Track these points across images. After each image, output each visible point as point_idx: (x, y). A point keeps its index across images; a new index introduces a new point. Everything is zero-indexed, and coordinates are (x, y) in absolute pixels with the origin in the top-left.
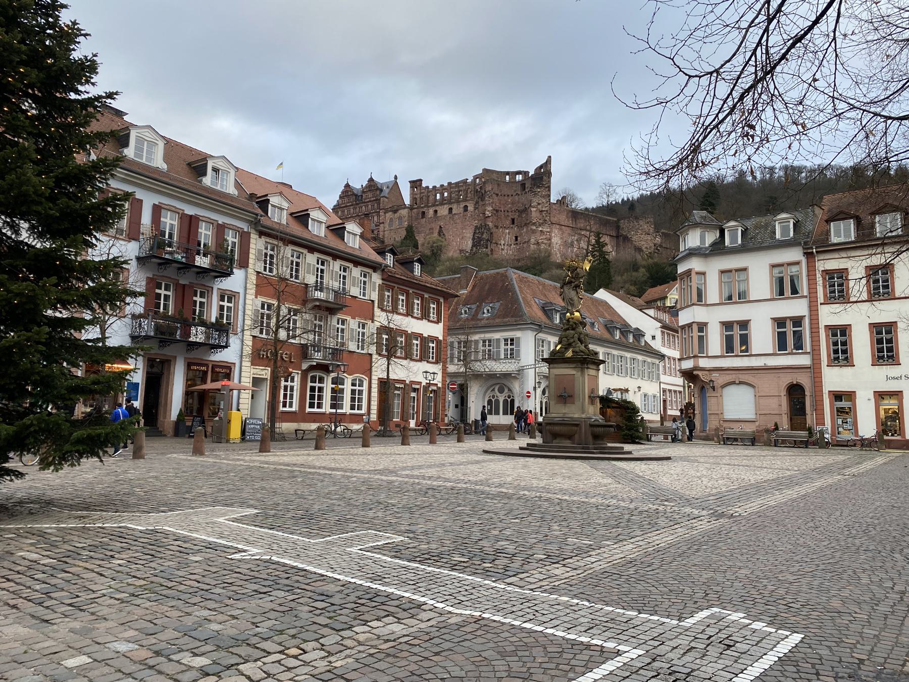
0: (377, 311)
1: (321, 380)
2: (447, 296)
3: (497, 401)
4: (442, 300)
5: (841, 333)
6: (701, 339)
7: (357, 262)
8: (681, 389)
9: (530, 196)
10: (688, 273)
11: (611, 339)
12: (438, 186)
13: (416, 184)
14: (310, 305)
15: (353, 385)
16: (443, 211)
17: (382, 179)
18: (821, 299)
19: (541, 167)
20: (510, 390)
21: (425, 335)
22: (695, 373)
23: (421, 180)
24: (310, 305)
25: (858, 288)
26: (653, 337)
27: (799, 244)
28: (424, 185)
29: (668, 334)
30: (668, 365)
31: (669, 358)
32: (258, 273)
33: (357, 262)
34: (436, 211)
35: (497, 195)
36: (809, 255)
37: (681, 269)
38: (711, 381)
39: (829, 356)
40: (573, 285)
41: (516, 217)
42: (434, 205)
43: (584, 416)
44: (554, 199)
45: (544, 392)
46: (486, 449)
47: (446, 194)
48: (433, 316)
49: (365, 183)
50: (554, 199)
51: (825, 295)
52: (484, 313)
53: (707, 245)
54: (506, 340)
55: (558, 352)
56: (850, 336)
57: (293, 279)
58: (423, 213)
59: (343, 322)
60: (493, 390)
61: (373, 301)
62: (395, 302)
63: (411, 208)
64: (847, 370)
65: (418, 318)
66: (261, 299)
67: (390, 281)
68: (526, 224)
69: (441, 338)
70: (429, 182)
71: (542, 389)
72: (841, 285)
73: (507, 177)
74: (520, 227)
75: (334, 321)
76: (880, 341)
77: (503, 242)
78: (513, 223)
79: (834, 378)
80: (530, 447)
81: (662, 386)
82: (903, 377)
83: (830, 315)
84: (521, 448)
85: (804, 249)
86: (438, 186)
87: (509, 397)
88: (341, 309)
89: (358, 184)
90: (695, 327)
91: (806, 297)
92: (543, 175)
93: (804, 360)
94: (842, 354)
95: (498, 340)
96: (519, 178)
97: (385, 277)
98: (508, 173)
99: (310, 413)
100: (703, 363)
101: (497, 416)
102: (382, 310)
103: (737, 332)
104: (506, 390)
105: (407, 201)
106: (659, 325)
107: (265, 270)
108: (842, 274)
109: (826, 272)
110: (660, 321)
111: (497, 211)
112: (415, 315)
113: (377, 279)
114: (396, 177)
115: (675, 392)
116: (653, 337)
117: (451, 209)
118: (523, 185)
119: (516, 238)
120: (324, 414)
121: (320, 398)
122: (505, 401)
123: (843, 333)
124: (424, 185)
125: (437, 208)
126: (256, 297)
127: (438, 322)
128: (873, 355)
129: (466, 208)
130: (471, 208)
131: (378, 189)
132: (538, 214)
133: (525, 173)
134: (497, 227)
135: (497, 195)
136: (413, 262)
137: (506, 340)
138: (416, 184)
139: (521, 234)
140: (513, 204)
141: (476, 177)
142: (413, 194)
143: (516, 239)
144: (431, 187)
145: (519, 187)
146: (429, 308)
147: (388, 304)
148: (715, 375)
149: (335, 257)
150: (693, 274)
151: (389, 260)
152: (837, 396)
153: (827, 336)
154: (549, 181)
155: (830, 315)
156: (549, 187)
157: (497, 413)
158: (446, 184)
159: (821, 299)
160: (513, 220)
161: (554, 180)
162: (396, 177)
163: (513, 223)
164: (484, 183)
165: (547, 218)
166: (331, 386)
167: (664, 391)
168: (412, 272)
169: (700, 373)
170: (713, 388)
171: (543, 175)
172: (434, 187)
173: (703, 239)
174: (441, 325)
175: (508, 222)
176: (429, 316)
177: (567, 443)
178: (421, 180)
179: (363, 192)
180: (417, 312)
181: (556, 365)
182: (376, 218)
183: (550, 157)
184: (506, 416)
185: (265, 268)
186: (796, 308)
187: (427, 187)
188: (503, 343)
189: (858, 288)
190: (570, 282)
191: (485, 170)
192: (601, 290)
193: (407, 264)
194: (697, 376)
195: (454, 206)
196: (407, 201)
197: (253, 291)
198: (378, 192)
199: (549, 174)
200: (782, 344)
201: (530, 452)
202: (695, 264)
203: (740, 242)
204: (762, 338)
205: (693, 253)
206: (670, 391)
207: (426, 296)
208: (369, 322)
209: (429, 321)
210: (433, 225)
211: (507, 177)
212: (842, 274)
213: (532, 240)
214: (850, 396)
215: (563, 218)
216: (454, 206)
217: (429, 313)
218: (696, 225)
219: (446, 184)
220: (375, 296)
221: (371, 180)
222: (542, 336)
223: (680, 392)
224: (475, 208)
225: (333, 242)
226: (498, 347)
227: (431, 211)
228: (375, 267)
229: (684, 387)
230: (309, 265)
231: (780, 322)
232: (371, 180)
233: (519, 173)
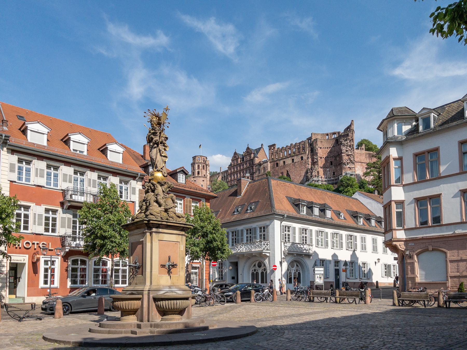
11: (298, 216)
16: (289, 161)
23: (274, 145)
34: (284, 162)
35: (321, 148)
41: (333, 160)
49: (245, 150)
58: (277, 164)
60: (255, 265)
74: (336, 166)
78: (332, 164)
89: (241, 151)
95: (255, 228)
104: (263, 265)
117: (293, 160)
119: (334, 173)
125: (285, 160)
130: (305, 158)
135: (321, 148)
136: (177, 173)
139: (337, 170)
143: (334, 174)
160: (331, 163)
163: (332, 164)
165: (352, 159)
182: (251, 171)
195: (295, 158)
210: (283, 170)
216: (295, 158)
221: (248, 148)
222: (284, 223)
227: (281, 163)
230: (65, 175)
232: (248, 148)
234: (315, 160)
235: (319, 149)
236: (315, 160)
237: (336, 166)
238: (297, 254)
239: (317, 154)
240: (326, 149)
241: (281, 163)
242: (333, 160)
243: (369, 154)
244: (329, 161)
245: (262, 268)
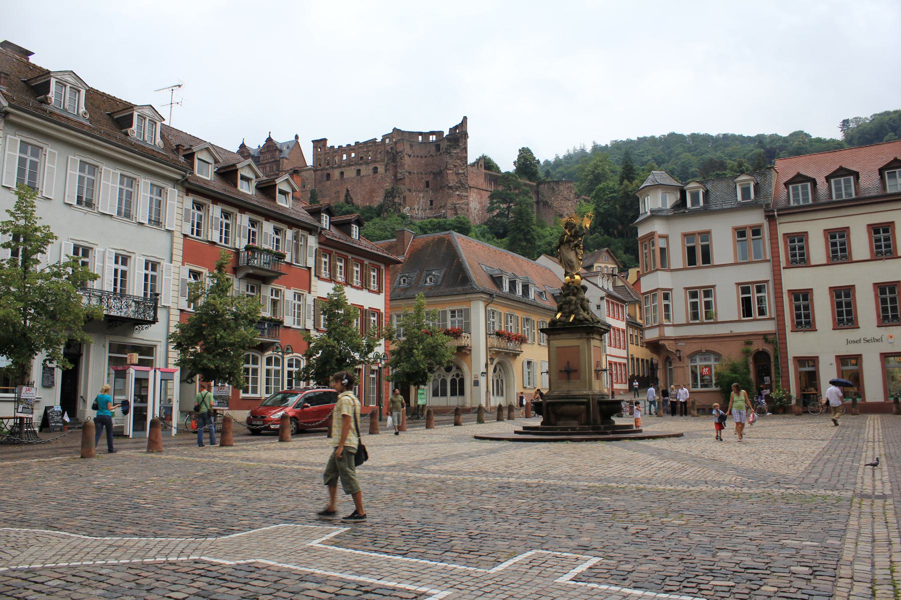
0: (313, 278)
1: (255, 361)
2: (388, 262)
3: (444, 382)
4: (383, 267)
5: (803, 297)
6: (667, 307)
7: (292, 223)
8: (625, 361)
9: (447, 158)
10: (652, 235)
12: (344, 146)
13: (320, 144)
14: (241, 275)
15: (290, 365)
16: (350, 173)
17: (281, 138)
18: (783, 263)
19: (456, 127)
20: (459, 368)
21: (366, 307)
22: (661, 342)
23: (325, 140)
24: (241, 275)
25: (817, 249)
26: (599, 307)
27: (760, 206)
28: (329, 145)
29: (613, 303)
30: (613, 337)
31: (614, 329)
32: (185, 236)
33: (292, 223)
34: (342, 173)
35: (410, 156)
36: (770, 218)
37: (642, 232)
38: (677, 350)
39: (792, 321)
40: (572, 244)
41: (430, 179)
42: (339, 167)
43: (590, 393)
44: (471, 158)
45: (495, 371)
46: (479, 434)
47: (353, 155)
48: (373, 286)
50: (471, 158)
51: (787, 260)
52: (426, 282)
53: (668, 207)
54: (453, 312)
55: (559, 320)
56: (812, 300)
57: (223, 243)
58: (328, 176)
59: (277, 292)
61: (310, 268)
62: (332, 270)
63: (315, 169)
64: (810, 335)
65: (357, 288)
66: (188, 267)
67: (327, 246)
68: (442, 188)
69: (383, 311)
70: (333, 142)
71: (493, 366)
72: (801, 248)
73: (420, 138)
75: (266, 292)
76: (839, 305)
77: (416, 207)
78: (428, 186)
79: (798, 344)
80: (528, 430)
81: (609, 358)
82: (862, 341)
83: (794, 279)
84: (516, 432)
85: (765, 211)
86: (344, 146)
87: (458, 375)
88: (276, 277)
90: (660, 295)
91: (769, 261)
92: (459, 135)
93: (768, 327)
94: (805, 321)
96: (433, 138)
97: (323, 240)
98: (420, 133)
99: (244, 399)
100: (669, 332)
101: (444, 398)
102: (319, 278)
103: (701, 300)
104: (454, 369)
105: (309, 162)
106: (603, 294)
107: (192, 233)
108: (802, 237)
109: (786, 235)
110: (602, 289)
111: (410, 173)
112: (355, 284)
113: (312, 242)
114: (297, 137)
115: (620, 364)
116: (599, 307)
117: (359, 171)
118: (437, 145)
119: (431, 202)
120: (258, 400)
121: (255, 381)
122: (453, 382)
123: (805, 298)
124: (329, 145)
125: (343, 170)
126: (183, 265)
127: (379, 292)
128: (834, 320)
129: (375, 169)
130: (381, 169)
131: (277, 149)
132: (455, 178)
133: (440, 133)
134: (410, 190)
135: (410, 156)
137: (453, 312)
138: (320, 144)
140: (426, 165)
141: (385, 137)
142: (316, 155)
143: (431, 203)
144: (336, 147)
145: (434, 148)
146: (370, 275)
147: (324, 274)
148: (681, 344)
149: (269, 217)
150: (656, 237)
151: (325, 221)
152: (801, 361)
153: (790, 301)
154: (466, 143)
155: (794, 279)
156: (466, 149)
157: (444, 394)
158: (353, 144)
159: (783, 263)
161: (470, 141)
162: (297, 137)
164: (396, 142)
166: (265, 367)
167: (610, 364)
168: (350, 234)
169: (666, 343)
170: (680, 358)
171: (459, 135)
172: (340, 147)
173: (664, 202)
174: (383, 295)
175: (422, 186)
176: (370, 286)
177: (574, 424)
178: (325, 140)
179: (261, 152)
180: (356, 281)
181: (557, 336)
183: (465, 118)
184: (454, 398)
185: (193, 230)
186: (761, 272)
187: (332, 147)
188: (449, 315)
189: (817, 249)
190: (569, 242)
191: (395, 129)
192: (543, 257)
193: (343, 227)
194: (664, 346)
196: (309, 162)
197: (180, 259)
198: (277, 153)
199: (465, 135)
200: (747, 310)
201: (528, 435)
202: (658, 227)
203: (701, 204)
204: (727, 305)
205: (655, 215)
206: (615, 363)
207: (366, 262)
208: (306, 293)
209: (370, 291)
211: (420, 138)
212: (802, 237)
213: (449, 205)
214: (814, 360)
215: (481, 182)
217: (370, 281)
218: (657, 186)
219: (353, 144)
220: (311, 263)
221: (269, 140)
223: (625, 365)
224: (386, 170)
225: (262, 202)
226: (445, 320)
227: (336, 174)
228: (311, 230)
229: (627, 359)
231: (745, 289)
232: (269, 140)
233: (432, 133)
234: (399, 176)
235: (406, 157)
236: (399, 176)
237: (435, 190)
238: (507, 354)
239: (402, 165)
240: (419, 159)
241: (336, 174)
242: (430, 179)
243: (490, 175)
244: (423, 181)
245: (454, 371)
